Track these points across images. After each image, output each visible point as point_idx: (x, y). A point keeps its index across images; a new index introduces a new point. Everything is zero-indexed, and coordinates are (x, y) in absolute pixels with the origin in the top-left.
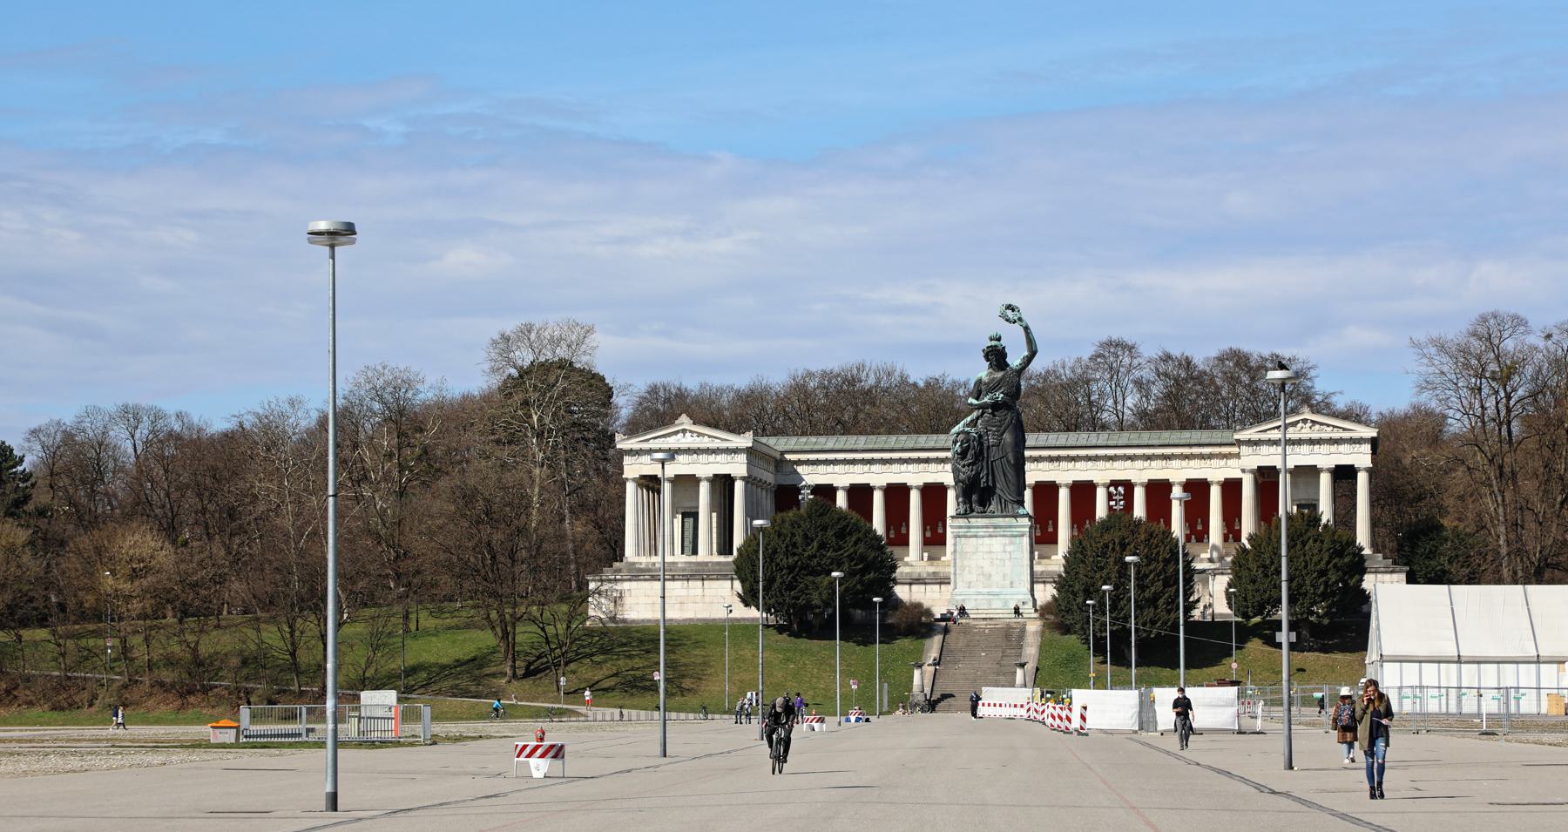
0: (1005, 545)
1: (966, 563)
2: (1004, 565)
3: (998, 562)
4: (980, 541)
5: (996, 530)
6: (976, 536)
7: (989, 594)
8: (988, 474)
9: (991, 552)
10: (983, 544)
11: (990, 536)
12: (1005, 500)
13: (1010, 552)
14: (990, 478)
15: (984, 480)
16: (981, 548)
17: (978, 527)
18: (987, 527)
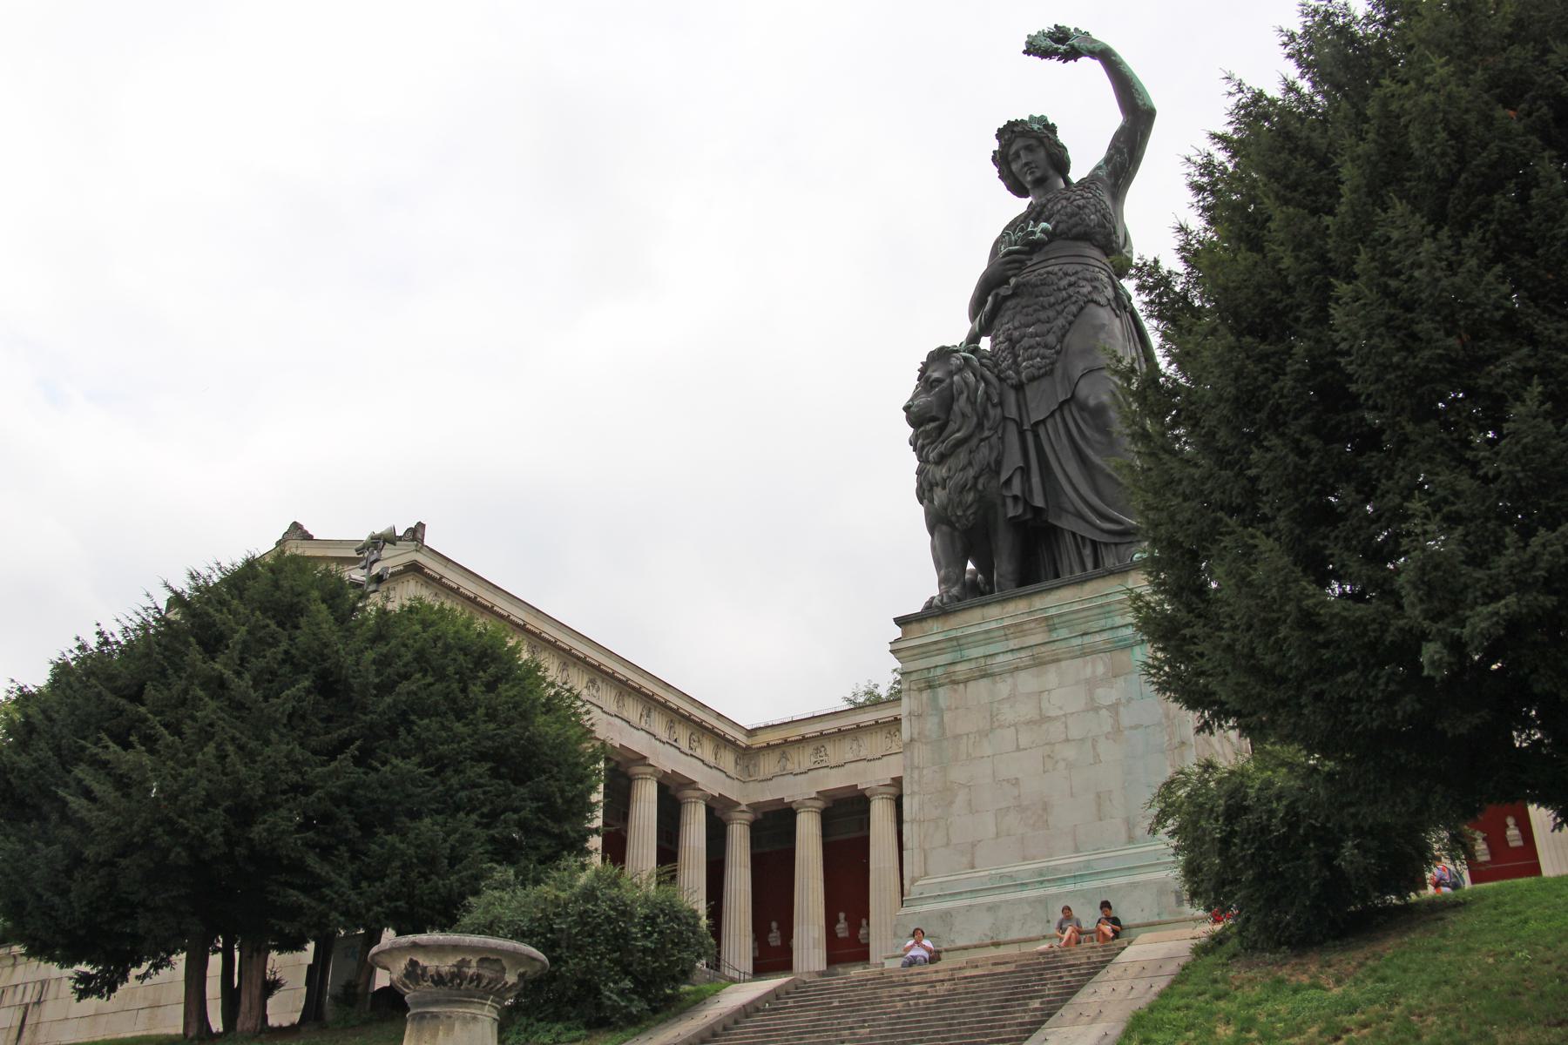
0: (1091, 684)
1: (957, 774)
2: (1097, 759)
3: (1070, 752)
4: (1003, 687)
5: (1054, 636)
6: (985, 675)
7: (1043, 879)
8: (1025, 471)
9: (1044, 719)
10: (1012, 697)
11: (1039, 663)
12: (1094, 544)
13: (1114, 708)
14: (1036, 480)
15: (1016, 488)
16: (1008, 714)
17: (988, 635)
18: (1019, 629)
